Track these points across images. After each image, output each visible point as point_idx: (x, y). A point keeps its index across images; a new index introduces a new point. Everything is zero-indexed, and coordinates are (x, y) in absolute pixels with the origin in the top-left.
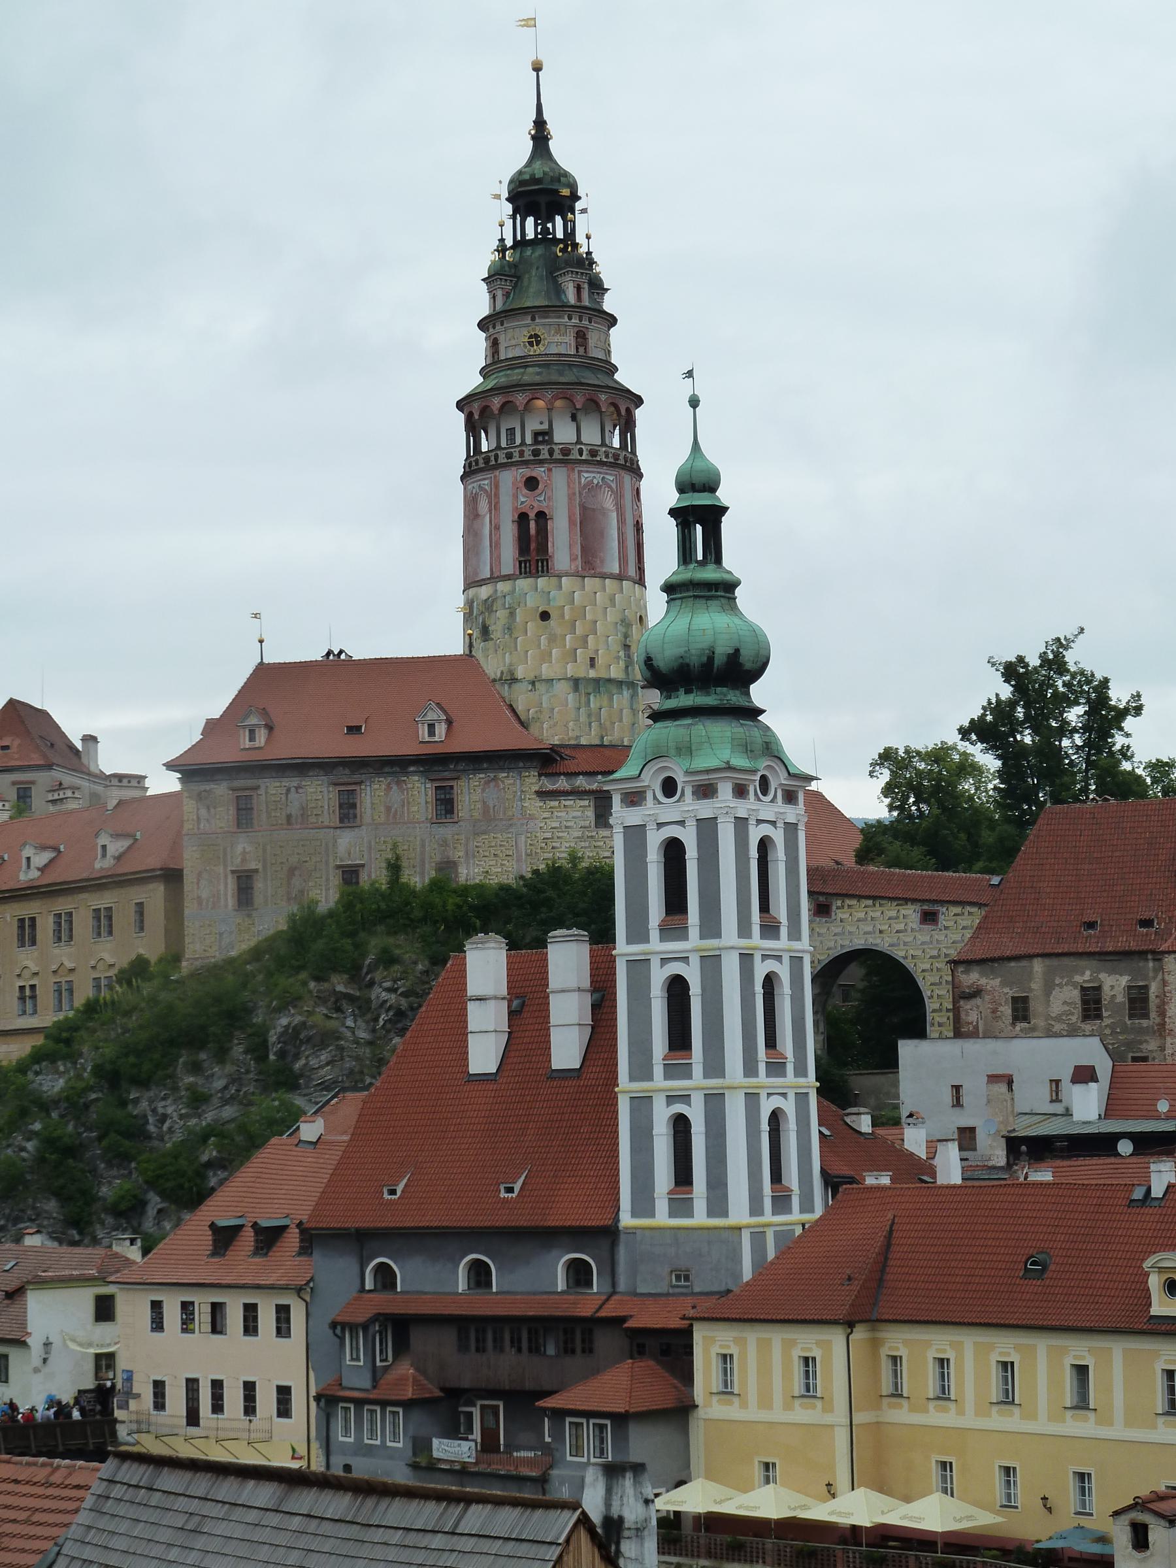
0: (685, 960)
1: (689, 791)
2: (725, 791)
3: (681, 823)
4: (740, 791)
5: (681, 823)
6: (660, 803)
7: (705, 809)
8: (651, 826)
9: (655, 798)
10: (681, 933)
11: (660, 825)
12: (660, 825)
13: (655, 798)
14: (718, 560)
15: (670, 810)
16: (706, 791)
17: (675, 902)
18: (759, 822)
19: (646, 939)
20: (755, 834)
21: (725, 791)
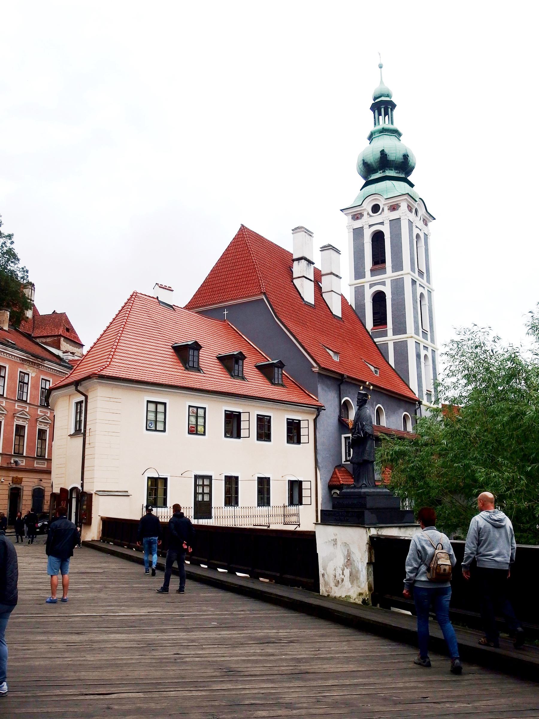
0: (383, 283)
1: (386, 209)
2: (404, 206)
3: (382, 223)
4: (410, 209)
5: (382, 223)
6: (371, 216)
7: (394, 215)
8: (366, 228)
9: (368, 214)
10: (383, 271)
11: (370, 226)
12: (370, 226)
13: (368, 214)
14: (392, 123)
15: (377, 218)
16: (394, 208)
17: (379, 259)
18: (417, 227)
19: (364, 276)
20: (416, 231)
21: (404, 206)
